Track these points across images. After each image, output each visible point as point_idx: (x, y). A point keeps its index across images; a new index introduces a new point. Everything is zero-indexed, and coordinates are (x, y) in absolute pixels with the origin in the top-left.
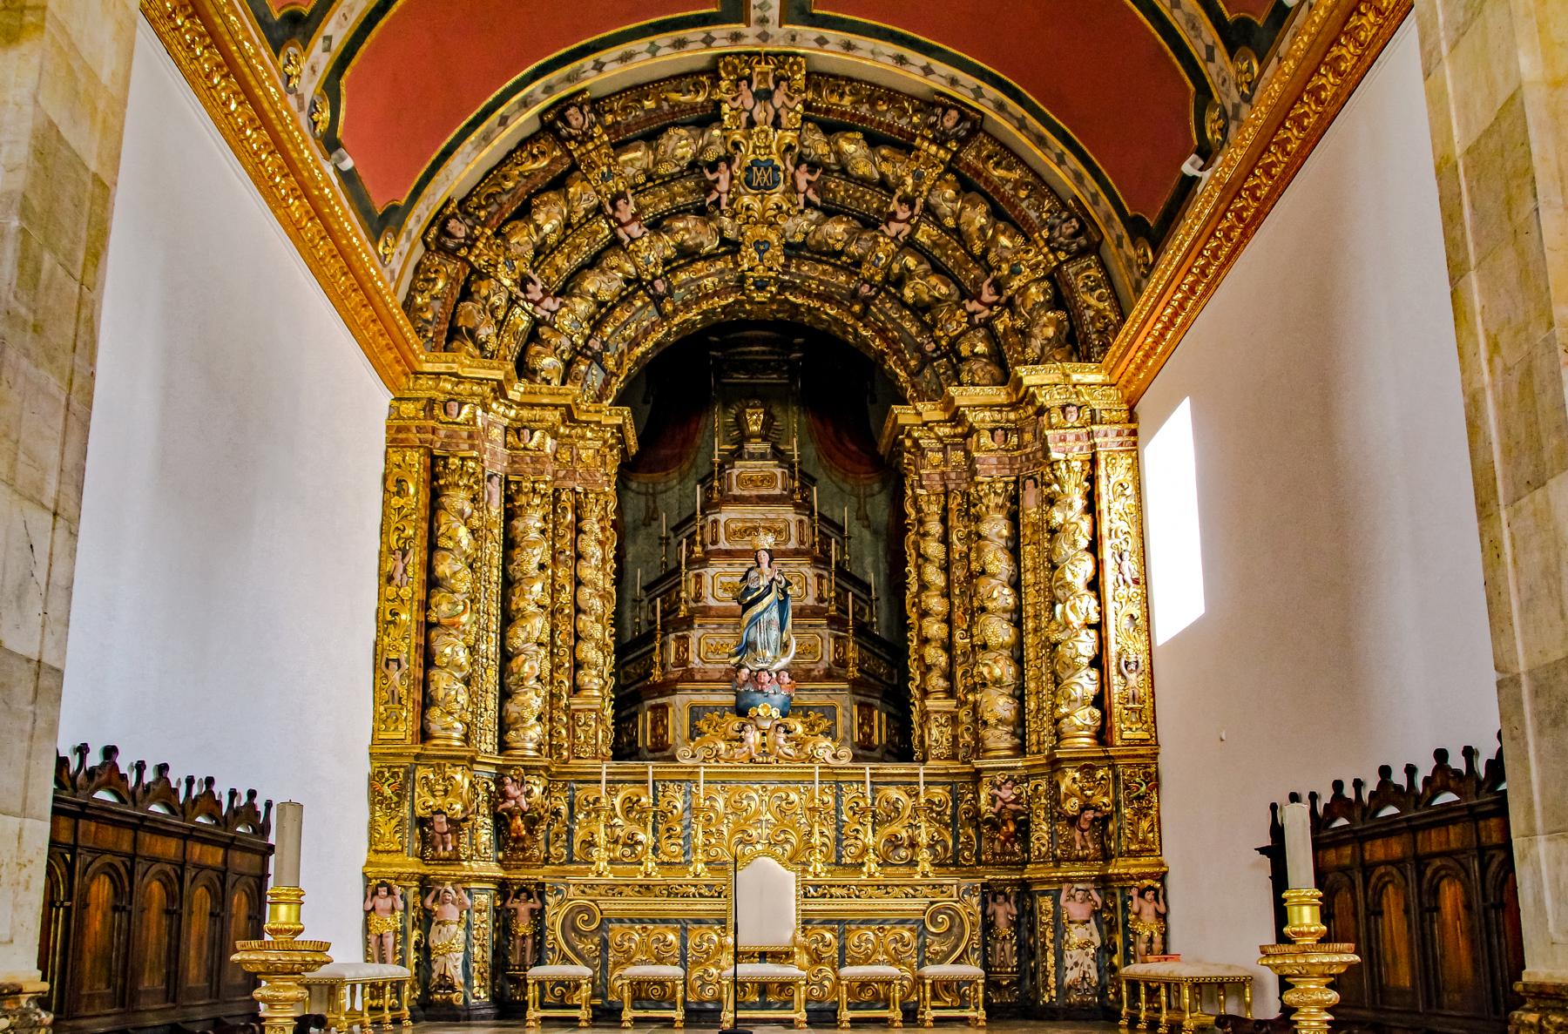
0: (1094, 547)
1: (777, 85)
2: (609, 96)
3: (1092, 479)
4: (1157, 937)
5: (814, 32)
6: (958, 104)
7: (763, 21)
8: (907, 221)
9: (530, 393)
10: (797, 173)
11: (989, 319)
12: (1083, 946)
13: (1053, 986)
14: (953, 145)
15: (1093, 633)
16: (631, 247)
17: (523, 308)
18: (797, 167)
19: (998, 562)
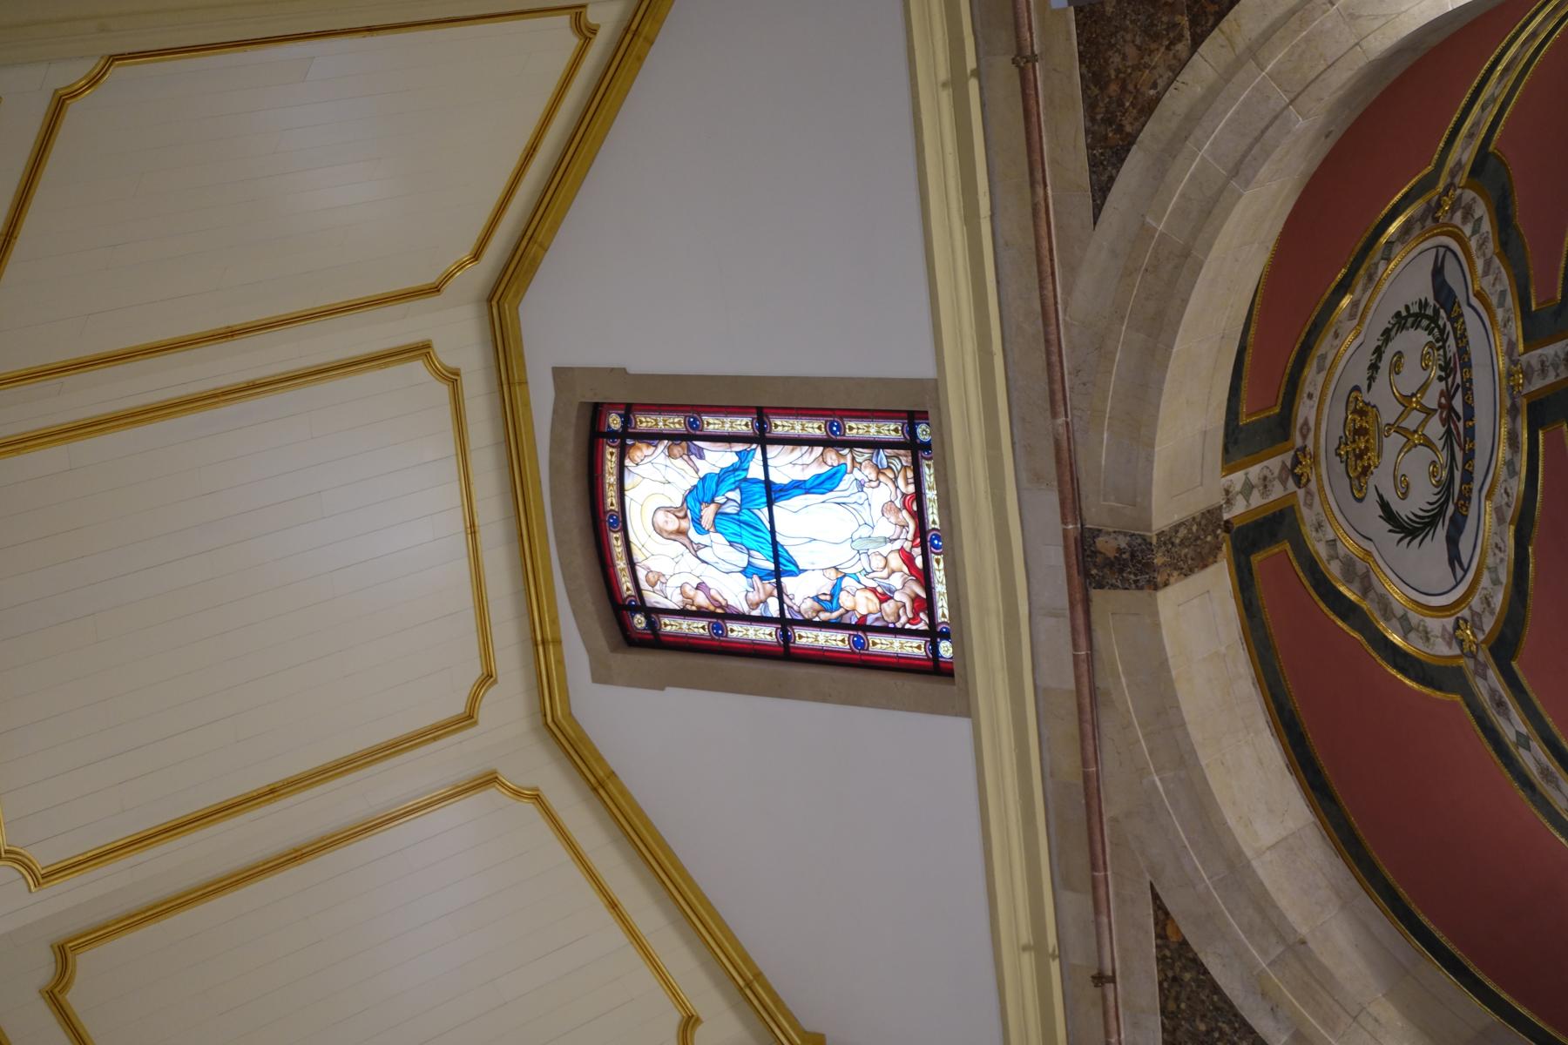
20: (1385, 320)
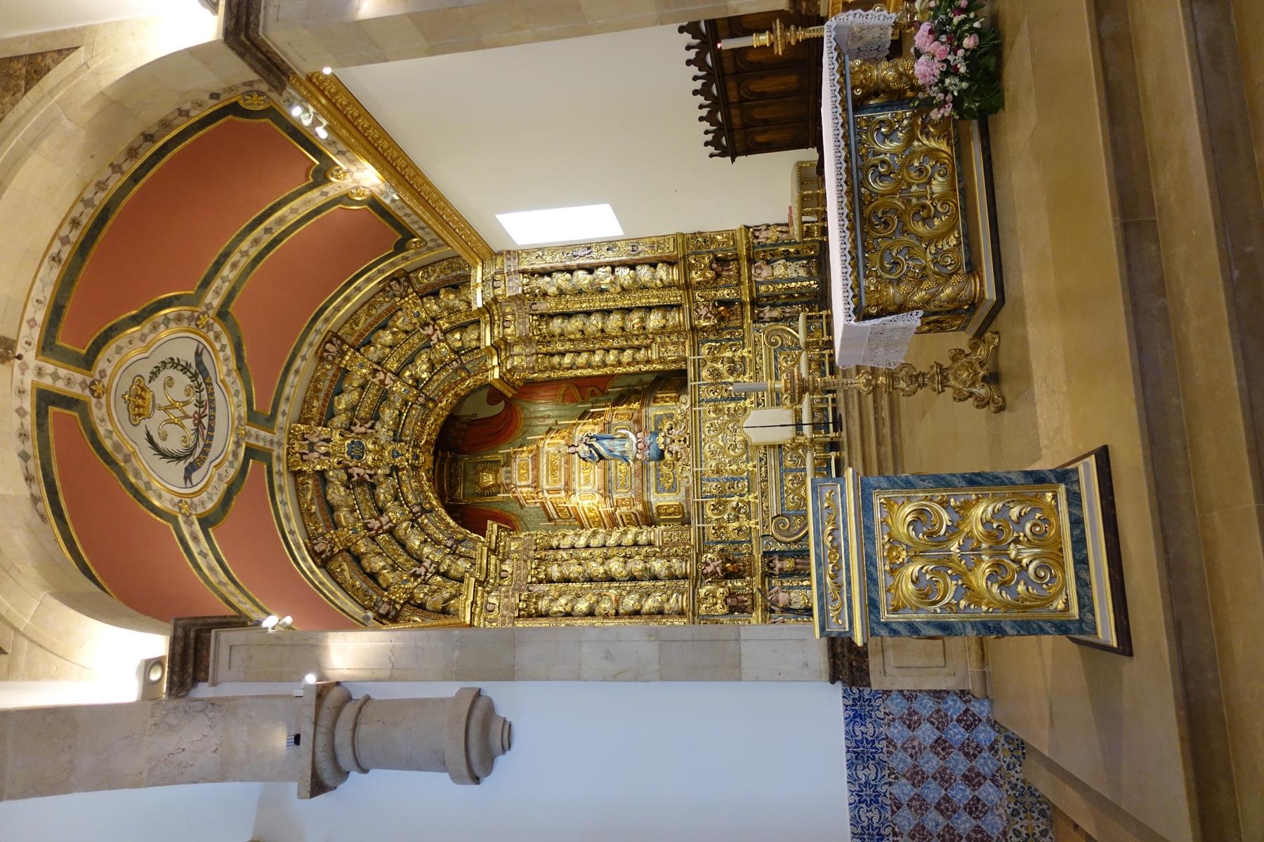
0: (570, 271)
1: (305, 440)
2: (307, 531)
3: (533, 273)
4: (779, 229)
5: (280, 418)
6: (325, 341)
7: (272, 442)
8: (385, 374)
9: (480, 570)
11: (442, 331)
12: (786, 268)
14: (345, 347)
15: (617, 269)
16: (394, 522)
17: (430, 578)
18: (352, 432)
19: (576, 323)
20: (165, 357)
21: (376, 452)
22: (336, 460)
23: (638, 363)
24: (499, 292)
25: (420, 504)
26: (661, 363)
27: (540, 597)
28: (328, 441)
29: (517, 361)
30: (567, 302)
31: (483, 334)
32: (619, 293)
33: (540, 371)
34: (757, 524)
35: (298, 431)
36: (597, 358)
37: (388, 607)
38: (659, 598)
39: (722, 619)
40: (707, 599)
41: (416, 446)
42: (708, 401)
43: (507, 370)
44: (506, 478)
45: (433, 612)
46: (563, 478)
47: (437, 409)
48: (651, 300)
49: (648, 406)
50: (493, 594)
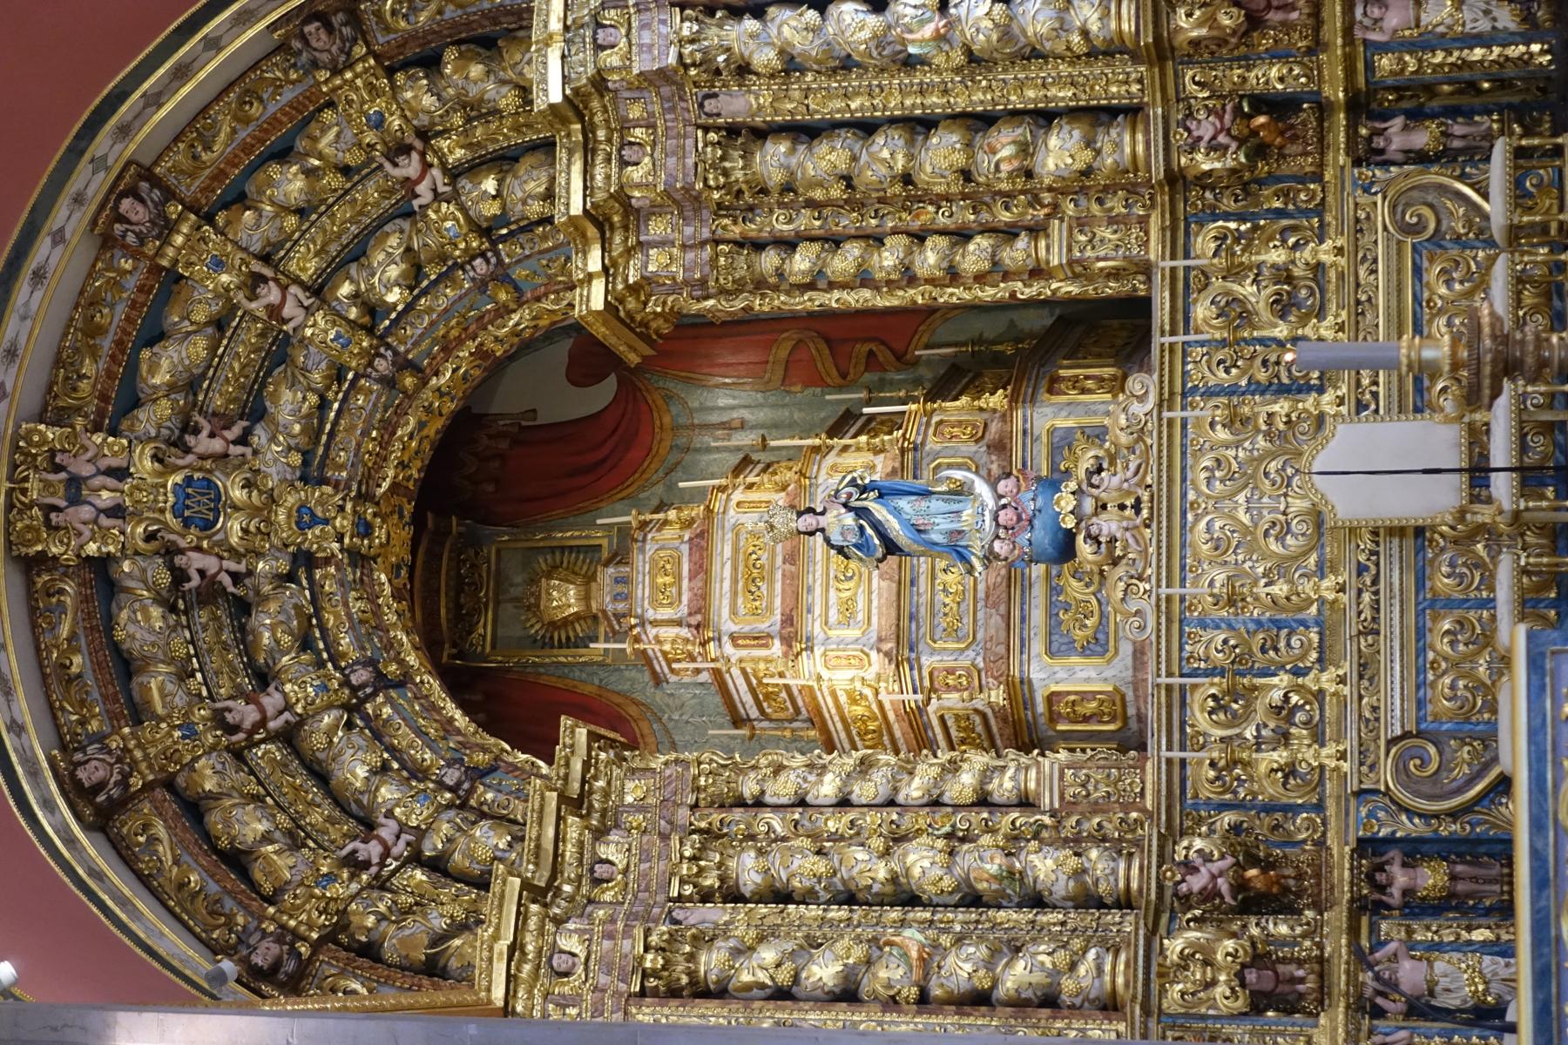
1: (58, 468)
2: (58, 727)
6: (117, 193)
8: (284, 289)
9: (537, 856)
10: (200, 449)
13: (1522, 48)
14: (174, 210)
16: (299, 710)
17: (393, 873)
18: (188, 450)
19: (829, 157)
21: (254, 511)
22: (140, 530)
23: (1007, 276)
24: (612, 59)
25: (371, 663)
26: (1076, 277)
27: (703, 940)
28: (121, 473)
29: (656, 261)
30: (807, 92)
31: (561, 179)
32: (958, 70)
33: (723, 292)
34: (1342, 756)
35: (38, 445)
36: (888, 259)
37: (275, 949)
38: (1047, 960)
39: (1228, 1029)
40: (1186, 968)
41: (364, 497)
42: (1209, 393)
43: (628, 287)
44: (616, 598)
45: (403, 969)
46: (778, 602)
47: (427, 395)
48: (1053, 92)
49: (1033, 401)
50: (571, 926)
